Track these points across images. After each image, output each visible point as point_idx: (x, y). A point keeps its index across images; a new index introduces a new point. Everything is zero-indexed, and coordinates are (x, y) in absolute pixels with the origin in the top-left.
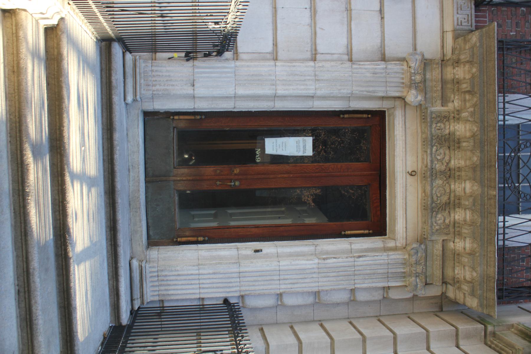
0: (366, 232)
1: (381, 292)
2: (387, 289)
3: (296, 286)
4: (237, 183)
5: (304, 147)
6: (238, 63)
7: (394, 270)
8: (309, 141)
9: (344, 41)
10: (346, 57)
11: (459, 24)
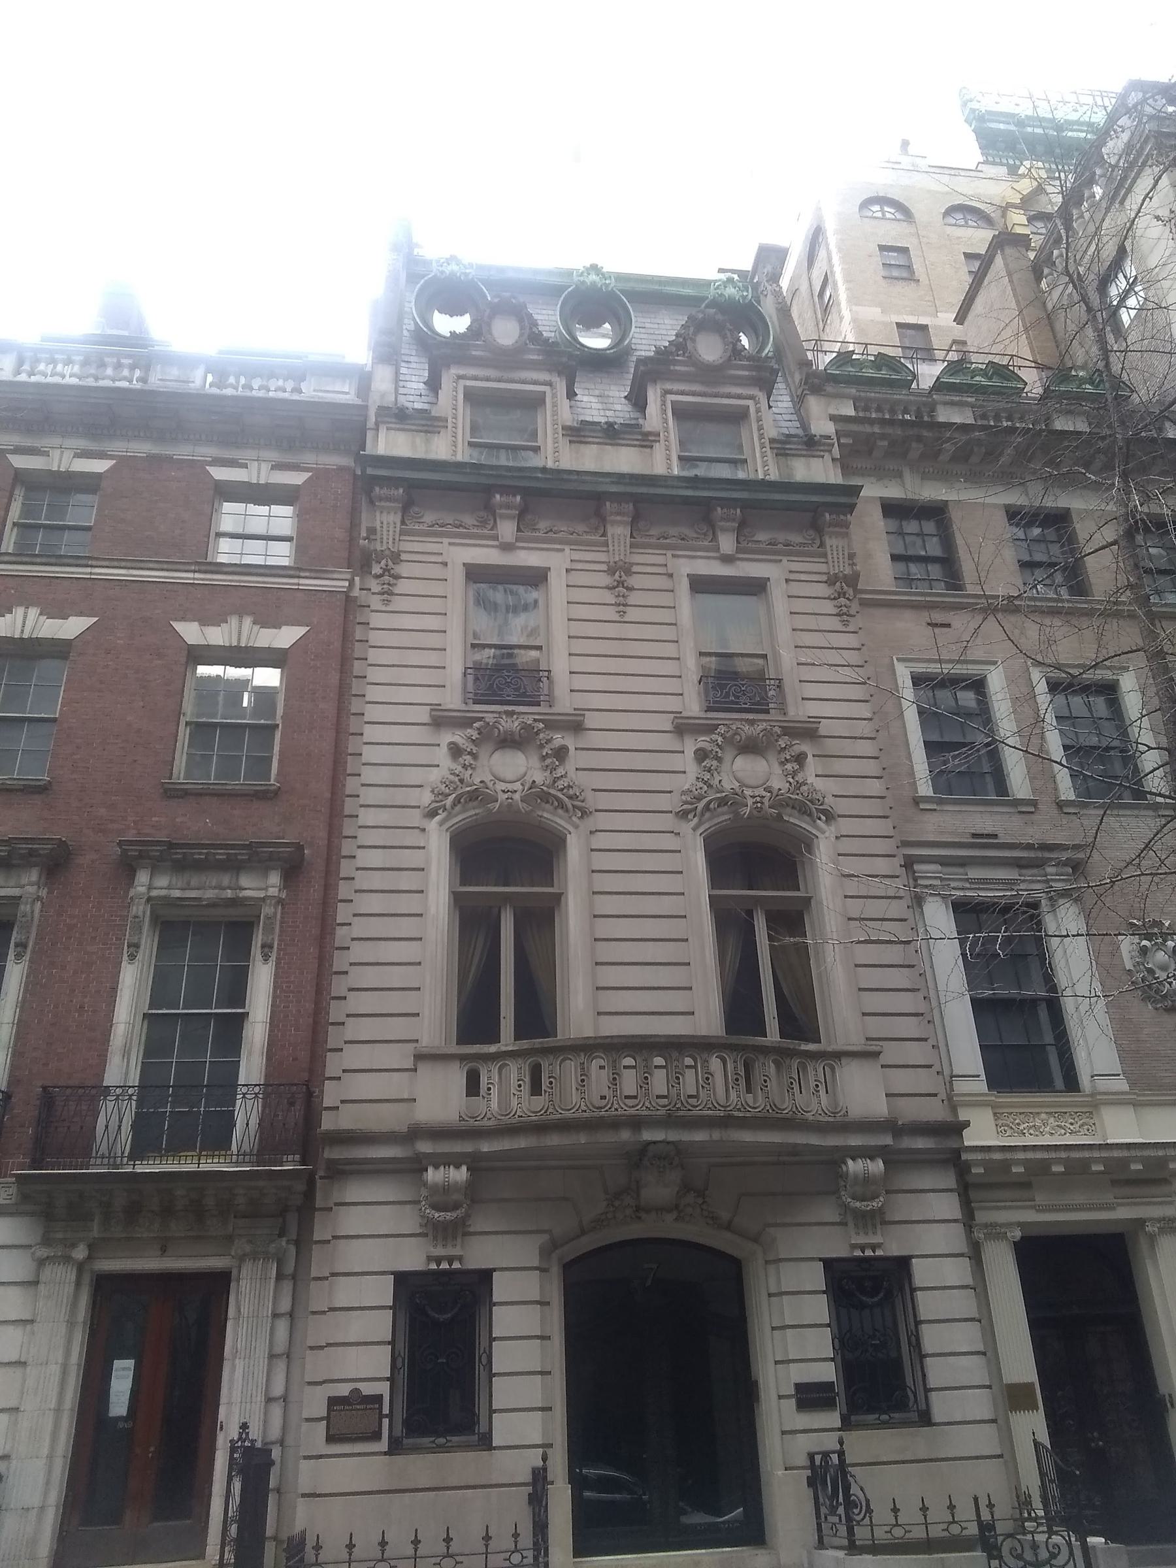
0: (225, 1296)
1: (286, 1282)
2: (280, 1277)
3: (260, 1384)
4: (152, 1449)
5: (124, 1369)
6: (13, 1456)
7: (259, 1273)
8: (117, 1364)
9: (10, 1329)
10: (29, 1327)
11: (9, 1197)
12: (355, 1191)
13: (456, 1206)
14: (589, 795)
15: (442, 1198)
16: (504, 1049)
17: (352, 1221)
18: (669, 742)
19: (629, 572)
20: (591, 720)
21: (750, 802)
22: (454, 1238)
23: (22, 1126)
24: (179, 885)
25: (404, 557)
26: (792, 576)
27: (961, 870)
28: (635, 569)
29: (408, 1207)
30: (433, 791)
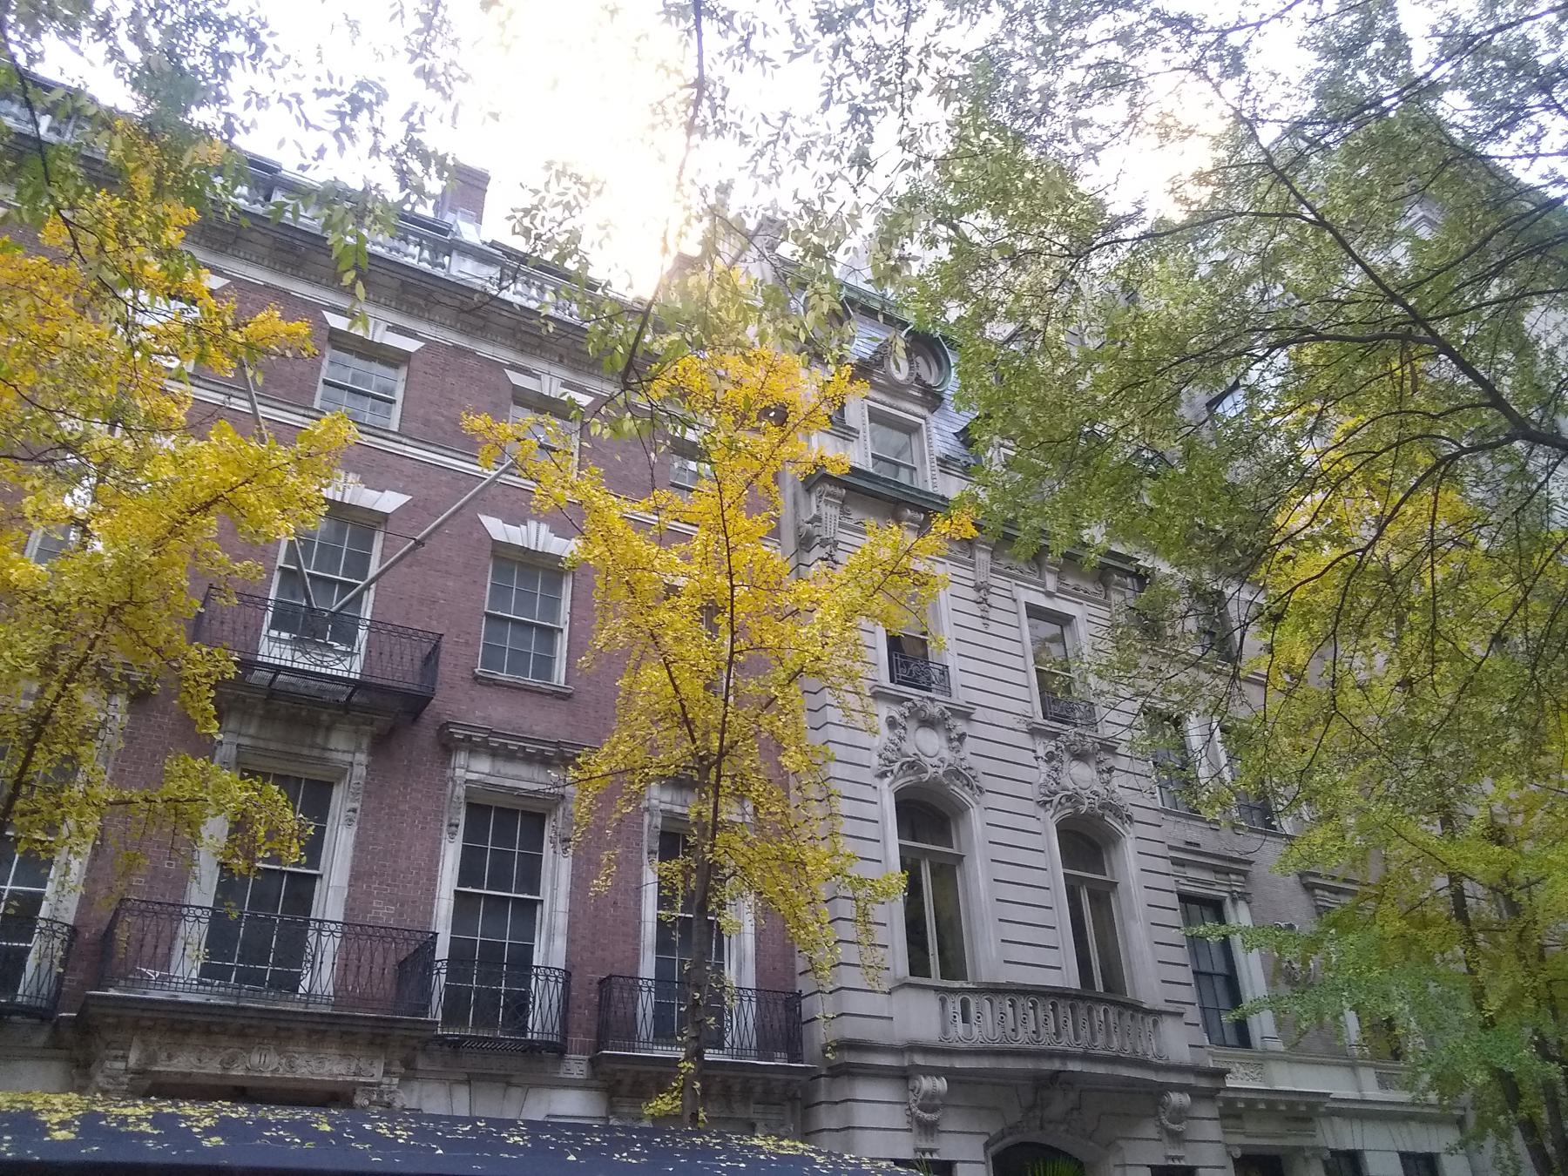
12: (865, 1089)
13: (933, 1110)
14: (981, 777)
15: (931, 1103)
16: (965, 986)
17: (863, 1115)
18: (1025, 741)
19: (988, 592)
20: (978, 714)
21: (1087, 801)
22: (932, 1135)
23: (580, 1007)
24: (679, 802)
25: (840, 546)
26: (1091, 618)
27: (1182, 869)
28: (993, 590)
29: (898, 1106)
30: (880, 756)
